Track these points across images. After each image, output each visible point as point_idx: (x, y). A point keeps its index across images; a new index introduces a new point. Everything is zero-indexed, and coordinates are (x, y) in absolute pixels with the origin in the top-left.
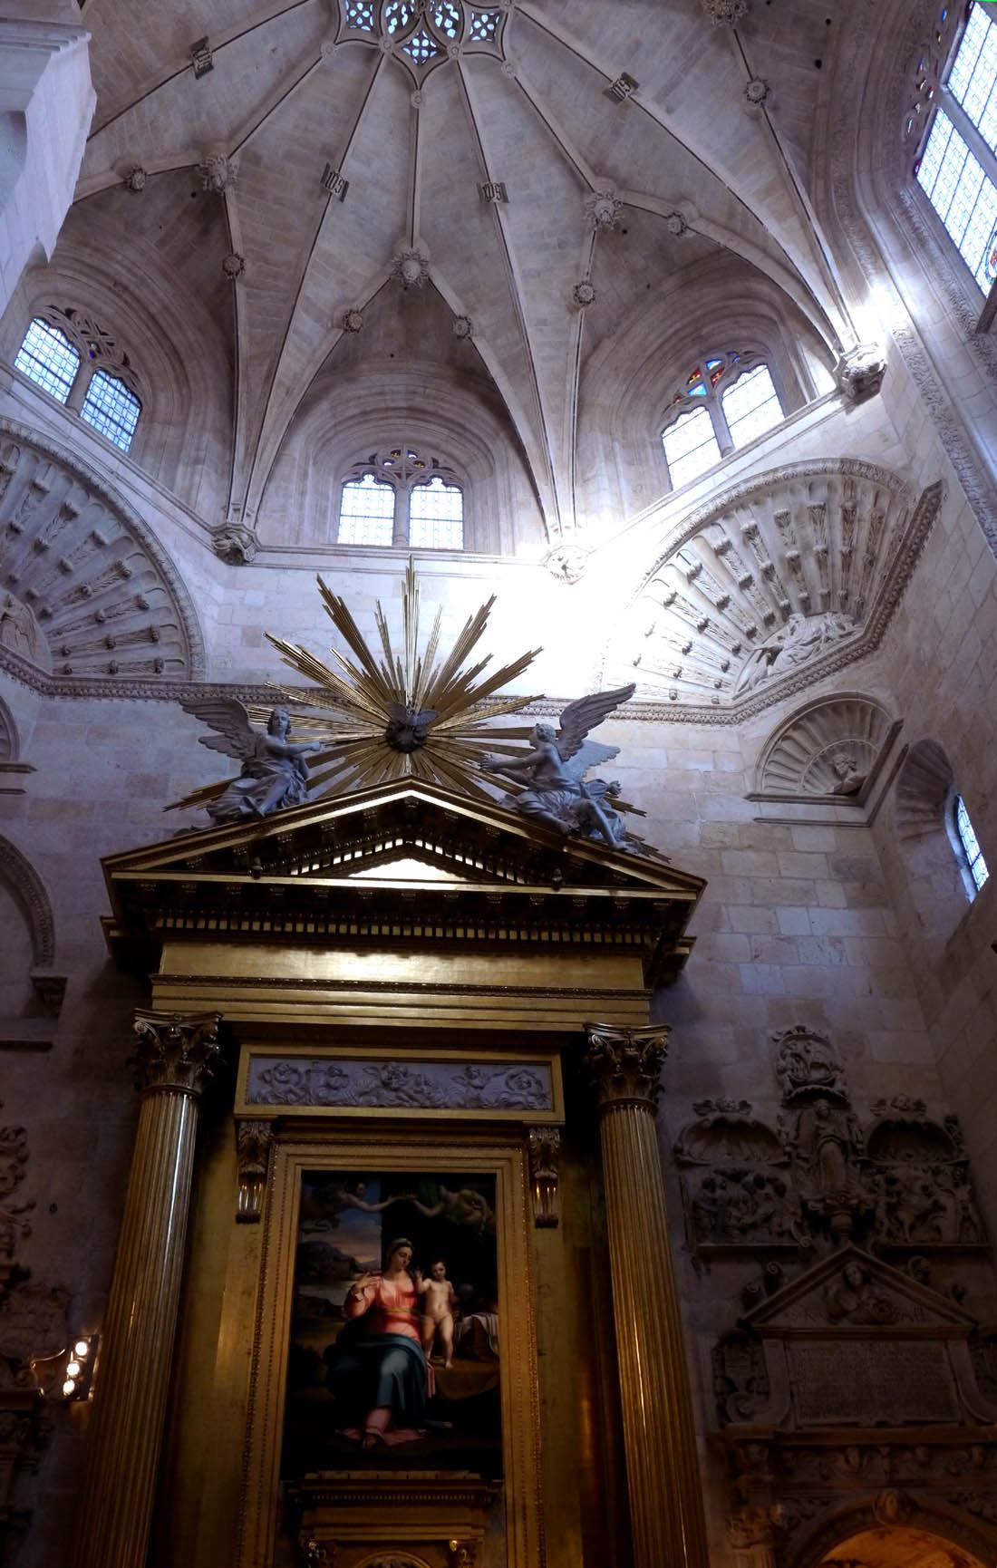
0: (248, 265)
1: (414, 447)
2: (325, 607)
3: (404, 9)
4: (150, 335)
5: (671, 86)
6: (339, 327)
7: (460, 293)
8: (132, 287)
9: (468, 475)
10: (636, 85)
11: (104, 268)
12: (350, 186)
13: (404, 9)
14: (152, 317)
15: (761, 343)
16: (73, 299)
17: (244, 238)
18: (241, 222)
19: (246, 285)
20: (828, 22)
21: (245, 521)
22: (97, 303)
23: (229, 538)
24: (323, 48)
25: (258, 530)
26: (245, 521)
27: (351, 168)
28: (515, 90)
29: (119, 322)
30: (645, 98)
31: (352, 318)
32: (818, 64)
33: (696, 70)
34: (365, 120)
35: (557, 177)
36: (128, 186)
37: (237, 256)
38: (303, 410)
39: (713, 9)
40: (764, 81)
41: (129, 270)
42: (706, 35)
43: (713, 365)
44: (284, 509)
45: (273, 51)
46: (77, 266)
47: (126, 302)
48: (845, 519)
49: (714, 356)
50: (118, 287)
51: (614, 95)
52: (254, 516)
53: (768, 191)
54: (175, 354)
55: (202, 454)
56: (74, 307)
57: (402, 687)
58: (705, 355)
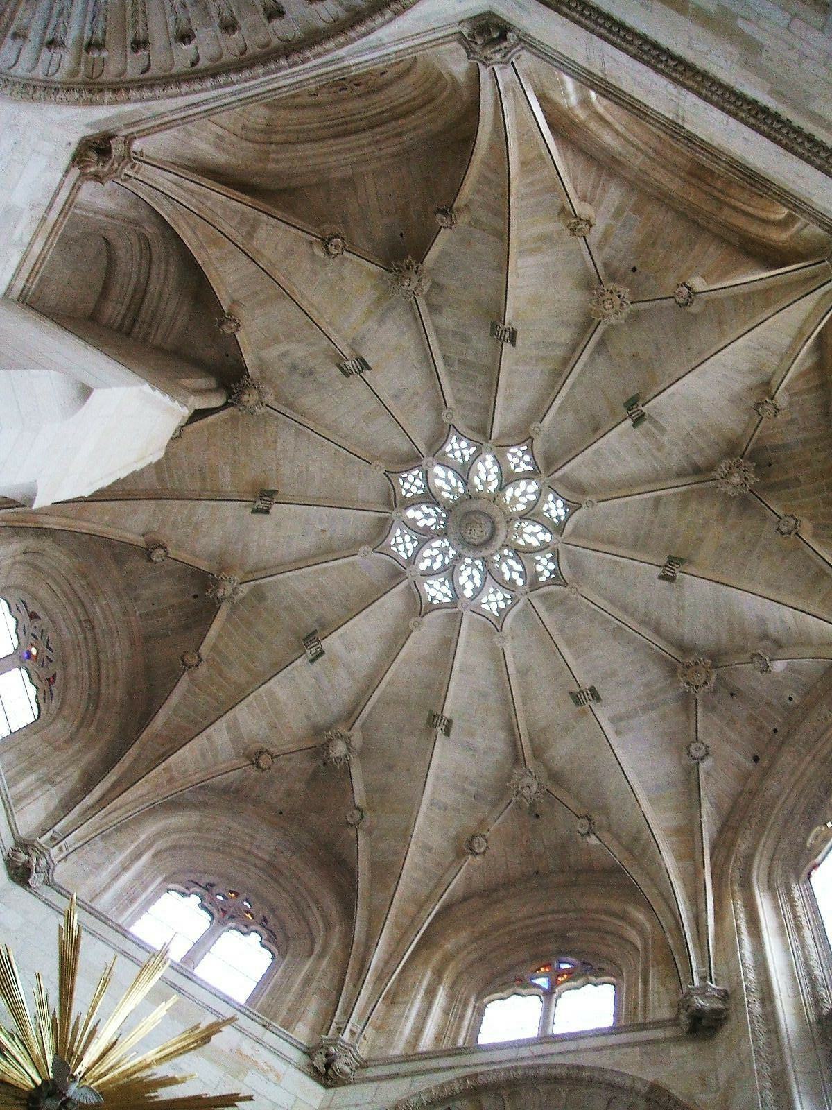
0: (203, 668)
1: (253, 899)
2: (60, 928)
4: (86, 673)
5: (628, 716)
6: (248, 757)
7: (368, 789)
8: (97, 630)
9: (287, 946)
11: (86, 602)
12: (324, 657)
14: (99, 662)
15: (618, 966)
16: (45, 609)
17: (214, 648)
18: (220, 636)
19: (192, 680)
20: (775, 731)
21: (54, 851)
22: (63, 625)
23: (27, 854)
24: (362, 549)
25: (59, 865)
26: (54, 851)
27: (332, 643)
28: (498, 658)
29: (69, 649)
30: (603, 714)
32: (756, 759)
33: (654, 714)
35: (500, 742)
36: (147, 553)
37: (199, 655)
38: (172, 805)
40: (706, 747)
41: (105, 617)
42: (672, 693)
43: (565, 966)
44: (98, 867)
45: (323, 531)
46: (66, 587)
47: (85, 638)
49: (570, 959)
50: (88, 623)
51: (576, 699)
52: (65, 853)
54: (95, 699)
55: (59, 779)
56: (41, 614)
57: (84, 1052)
58: (561, 954)
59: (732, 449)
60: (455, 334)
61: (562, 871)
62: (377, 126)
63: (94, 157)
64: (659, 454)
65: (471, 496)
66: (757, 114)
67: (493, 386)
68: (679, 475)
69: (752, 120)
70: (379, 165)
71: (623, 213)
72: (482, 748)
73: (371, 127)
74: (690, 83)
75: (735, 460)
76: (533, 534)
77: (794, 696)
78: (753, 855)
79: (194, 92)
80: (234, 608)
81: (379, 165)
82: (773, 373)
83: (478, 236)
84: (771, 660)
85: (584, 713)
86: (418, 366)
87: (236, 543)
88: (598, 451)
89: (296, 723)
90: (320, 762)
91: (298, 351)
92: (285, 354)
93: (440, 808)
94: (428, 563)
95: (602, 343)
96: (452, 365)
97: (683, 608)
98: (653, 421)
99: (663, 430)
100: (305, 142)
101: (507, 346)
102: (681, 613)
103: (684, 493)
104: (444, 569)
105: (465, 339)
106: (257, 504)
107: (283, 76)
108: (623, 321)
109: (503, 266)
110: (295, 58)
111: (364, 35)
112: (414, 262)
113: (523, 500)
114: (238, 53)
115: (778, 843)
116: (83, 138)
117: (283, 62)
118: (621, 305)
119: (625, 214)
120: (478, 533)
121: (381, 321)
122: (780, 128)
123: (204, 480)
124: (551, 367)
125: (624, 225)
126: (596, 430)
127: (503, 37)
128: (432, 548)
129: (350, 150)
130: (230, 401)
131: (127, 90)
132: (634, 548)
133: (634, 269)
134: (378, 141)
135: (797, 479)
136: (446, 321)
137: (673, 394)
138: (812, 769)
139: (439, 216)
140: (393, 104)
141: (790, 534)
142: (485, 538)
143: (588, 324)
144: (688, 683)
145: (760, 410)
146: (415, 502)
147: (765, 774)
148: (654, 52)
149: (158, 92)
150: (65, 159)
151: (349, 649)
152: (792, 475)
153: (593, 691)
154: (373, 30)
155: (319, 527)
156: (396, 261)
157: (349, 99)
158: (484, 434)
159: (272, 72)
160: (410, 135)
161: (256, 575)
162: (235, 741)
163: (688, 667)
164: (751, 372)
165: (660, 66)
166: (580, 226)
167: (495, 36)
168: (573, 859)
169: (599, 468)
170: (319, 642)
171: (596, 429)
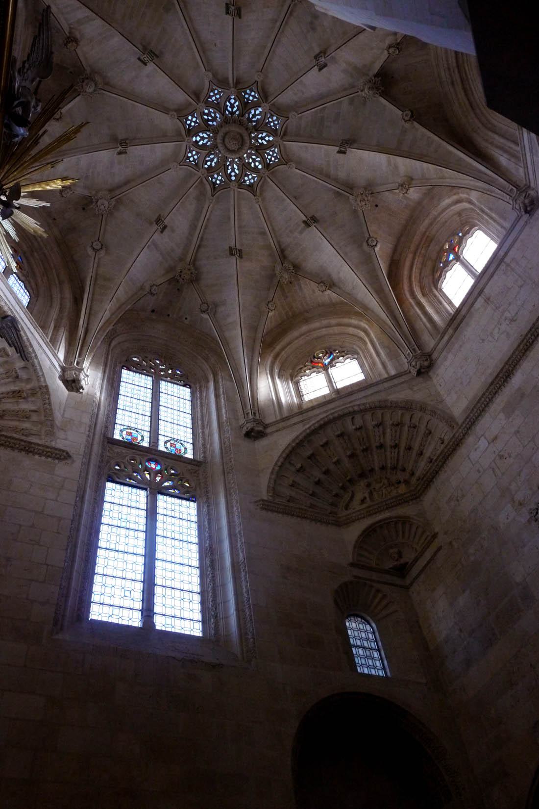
3: (210, 118)
10: (162, 232)
13: (210, 118)
20: (169, 315)
27: (151, 67)
32: (153, 311)
35: (118, 179)
45: (215, 45)
48: (14, 392)
51: (158, 220)
68: (279, 242)
69: (504, 370)
74: (521, 347)
75: (293, 271)
76: (234, 170)
88: (284, 200)
97: (215, 258)
99: (301, 232)
106: (232, 7)
109: (381, 149)
120: (233, 146)
126: (295, 198)
127: (526, 212)
139: (409, 113)
140: (470, 81)
141: (269, 309)
146: (239, 98)
151: (148, 76)
153: (165, 227)
156: (380, 80)
162: (80, 22)
170: (151, 61)
171: (295, 198)
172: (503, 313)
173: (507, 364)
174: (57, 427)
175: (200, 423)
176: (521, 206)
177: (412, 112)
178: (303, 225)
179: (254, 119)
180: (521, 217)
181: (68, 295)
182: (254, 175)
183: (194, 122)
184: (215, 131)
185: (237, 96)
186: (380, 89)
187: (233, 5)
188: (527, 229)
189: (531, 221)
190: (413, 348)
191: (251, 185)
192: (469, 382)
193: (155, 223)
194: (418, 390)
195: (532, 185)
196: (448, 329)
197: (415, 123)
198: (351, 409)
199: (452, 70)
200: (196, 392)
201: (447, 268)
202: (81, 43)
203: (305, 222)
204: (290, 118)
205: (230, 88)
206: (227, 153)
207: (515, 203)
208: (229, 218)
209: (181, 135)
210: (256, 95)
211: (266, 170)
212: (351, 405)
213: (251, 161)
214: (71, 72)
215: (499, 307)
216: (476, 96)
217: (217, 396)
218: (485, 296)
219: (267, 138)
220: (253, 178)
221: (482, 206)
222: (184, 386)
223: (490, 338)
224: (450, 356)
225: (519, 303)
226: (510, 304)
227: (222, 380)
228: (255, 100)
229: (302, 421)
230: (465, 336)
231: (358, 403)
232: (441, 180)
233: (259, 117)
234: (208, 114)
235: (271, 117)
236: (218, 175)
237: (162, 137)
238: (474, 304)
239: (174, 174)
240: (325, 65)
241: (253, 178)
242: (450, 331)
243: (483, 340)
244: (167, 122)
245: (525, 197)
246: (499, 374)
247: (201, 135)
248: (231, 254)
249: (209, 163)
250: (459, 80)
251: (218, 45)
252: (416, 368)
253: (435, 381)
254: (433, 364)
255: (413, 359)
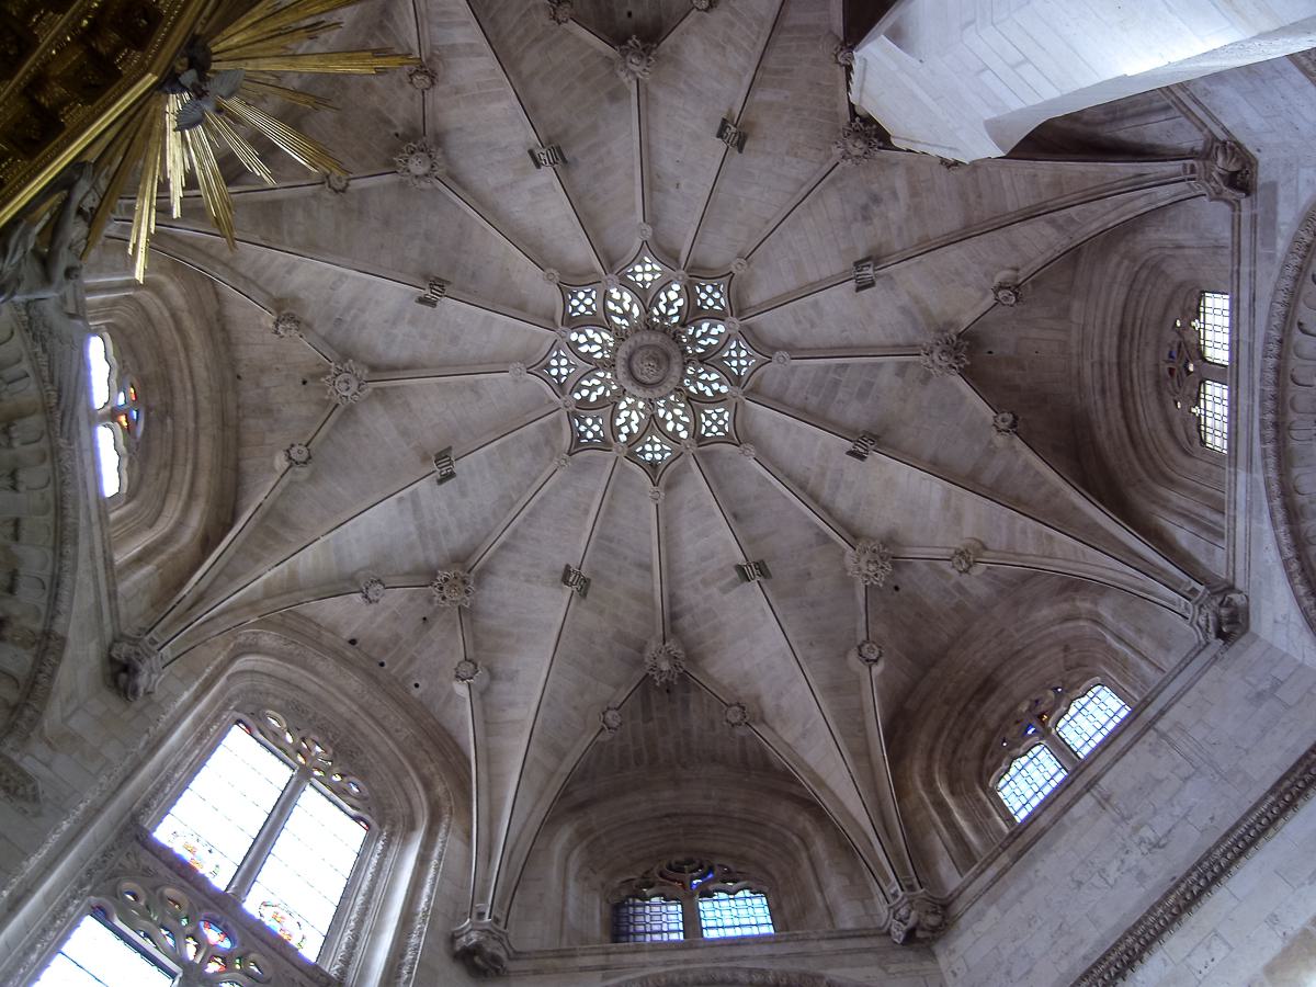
10: (440, 482)
17: (568, 33)
18: (579, 40)
20: (382, 664)
27: (547, 175)
28: (497, 364)
31: (427, 80)
32: (353, 642)
33: (414, 537)
34: (569, 217)
35: (397, 353)
39: (456, 578)
51: (443, 456)
53: (293, 575)
59: (693, 658)
60: (871, 385)
61: (238, 407)
62: (1119, 370)
63: (1233, 168)
64: (698, 578)
65: (674, 335)
66: (1128, 955)
67: (804, 414)
68: (672, 596)
69: (1122, 948)
70: (1074, 351)
71: (960, 593)
72: (395, 331)
73: (1119, 364)
74: (1172, 900)
75: (683, 664)
76: (630, 417)
77: (420, 690)
78: (258, 653)
79: (1270, 316)
80: (610, 62)
81: (1074, 351)
82: (773, 729)
83: (977, 448)
84: (469, 684)
85: (425, 459)
86: (844, 334)
87: (685, 82)
89: (454, 115)
90: (400, 130)
91: (896, 212)
92: (894, 194)
93: (334, 283)
94: (616, 296)
95: (826, 539)
96: (835, 371)
98: (734, 584)
99: (724, 591)
100: (1128, 295)
101: (849, 445)
102: (522, 578)
103: (652, 597)
104: (608, 313)
105: (862, 395)
107: (1253, 406)
108: (849, 574)
109: (937, 468)
110: (1270, 433)
111: (1272, 515)
112: (962, 366)
113: (669, 416)
114: (1294, 373)
115: (269, 675)
116: (1257, 163)
117: (1270, 417)
118: (867, 576)
119: (957, 595)
120: (646, 370)
121: (904, 310)
122: (1110, 973)
123: (777, 72)
124: (812, 481)
125: (945, 590)
126: (735, 516)
127: (1220, 634)
128: (631, 304)
129: (1102, 335)
130: (857, 119)
131: (1304, 257)
132: (600, 537)
133: (897, 588)
134: (1102, 365)
135: (651, 719)
136: (886, 377)
137: (765, 615)
138: (342, 709)
139: (1010, 417)
141: (604, 722)
142: (639, 376)
143: (854, 535)
144: (446, 580)
145: (737, 708)
146: (688, 292)
147: (338, 655)
148: (1209, 875)
149: (1287, 283)
150: (1242, 138)
151: (533, 191)
152: (655, 714)
153: (451, 475)
154: (1275, 527)
155: (683, 183)
156: (968, 347)
157: (1157, 352)
158: (751, 390)
159: (1262, 401)
160: (1100, 403)
161: (642, 98)
162: (453, 47)
163: (464, 582)
164: (778, 707)
165: (1194, 876)
166: (964, 562)
167: (1224, 629)
168: (252, 422)
169: (692, 510)
172: (1136, 830)
173: (1131, 934)
174: (42, 731)
175: (360, 900)
176: (1210, 617)
177: (1016, 418)
178: (735, 575)
179: (702, 342)
180: (1205, 647)
181: (195, 521)
182: (666, 448)
183: (586, 305)
184: (620, 336)
185: (686, 287)
186: (963, 362)
187: (735, 126)
188: (1215, 670)
189: (1226, 655)
190: (910, 883)
191: (653, 464)
192: (1028, 972)
193: (434, 458)
194: (899, 972)
195: (1239, 585)
196: (1000, 854)
197: (1018, 442)
198: (728, 975)
199: (1106, 367)
200: (378, 841)
201: (1017, 750)
202: (441, 87)
203: (740, 569)
204: (774, 361)
205: (679, 268)
206: (630, 382)
207: (1197, 611)
208: (586, 512)
209: (553, 320)
210: (722, 300)
211: (693, 441)
212: (733, 964)
213: (669, 416)
214: (397, 135)
215: (1130, 817)
216: (1144, 426)
217: (423, 861)
218: (1099, 792)
219: (716, 386)
220: (662, 452)
221: (1122, 625)
222: (356, 819)
223: (1096, 880)
224: (993, 912)
225: (1178, 811)
226: (1155, 812)
227: (447, 831)
228: (717, 308)
229: (604, 968)
230: (1036, 871)
231: (748, 964)
232: (1048, 561)
233: (714, 342)
234: (619, 303)
235: (738, 349)
236: (595, 422)
237: (519, 308)
238: (1071, 807)
239: (507, 388)
240: (872, 284)
241: (662, 452)
242: (1004, 859)
243: (1080, 884)
244: (537, 286)
245: (1222, 602)
246: (1108, 953)
247: (590, 332)
248: (565, 580)
249: (585, 393)
250: (1116, 390)
251: (682, 186)
252: (905, 924)
253: (943, 961)
254: (946, 924)
255: (903, 902)
